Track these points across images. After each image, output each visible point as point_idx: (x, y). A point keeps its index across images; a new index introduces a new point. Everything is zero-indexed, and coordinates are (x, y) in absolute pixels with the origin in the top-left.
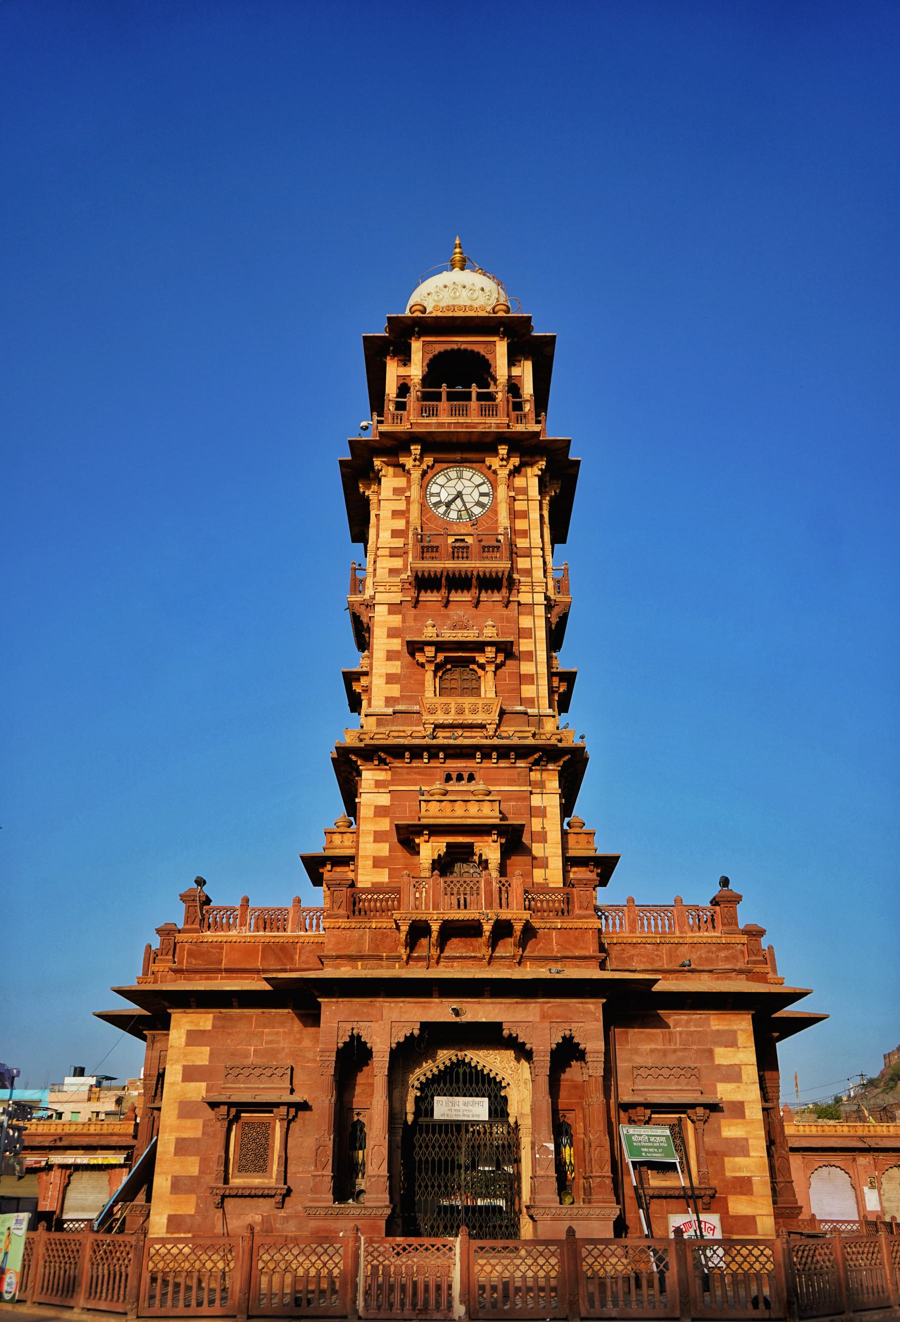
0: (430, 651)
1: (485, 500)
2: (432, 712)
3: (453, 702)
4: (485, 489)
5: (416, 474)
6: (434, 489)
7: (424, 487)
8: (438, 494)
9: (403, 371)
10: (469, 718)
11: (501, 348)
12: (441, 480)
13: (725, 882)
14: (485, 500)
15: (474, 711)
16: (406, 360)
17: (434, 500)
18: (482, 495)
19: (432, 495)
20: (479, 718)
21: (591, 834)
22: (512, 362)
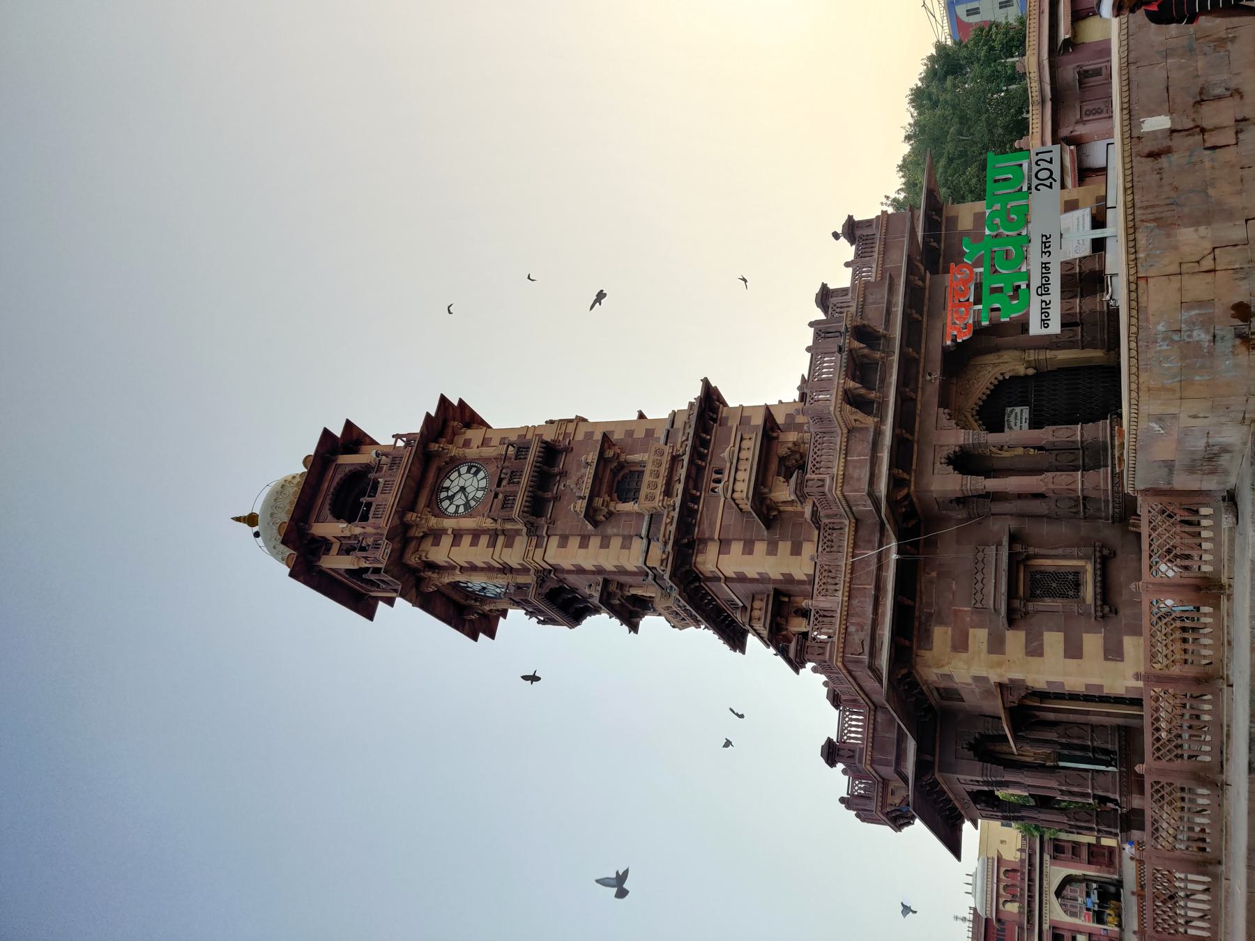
1: (474, 470)
4: (464, 469)
5: (433, 521)
7: (449, 517)
8: (458, 507)
13: (836, 236)
18: (468, 471)
19: (456, 512)
20: (666, 459)
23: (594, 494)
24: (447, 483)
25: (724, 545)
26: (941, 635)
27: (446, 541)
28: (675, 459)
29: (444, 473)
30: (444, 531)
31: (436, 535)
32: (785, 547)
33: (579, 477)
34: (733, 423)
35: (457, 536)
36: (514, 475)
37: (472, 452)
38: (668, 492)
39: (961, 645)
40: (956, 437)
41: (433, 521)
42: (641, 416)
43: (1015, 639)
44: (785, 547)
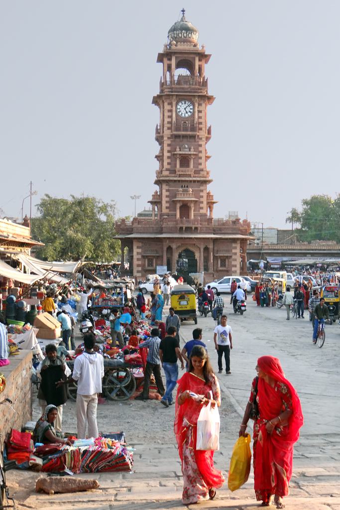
0: (178, 156)
1: (191, 111)
2: (179, 171)
3: (183, 169)
5: (174, 103)
6: (179, 107)
9: (169, 62)
10: (187, 173)
11: (197, 59)
12: (180, 104)
14: (191, 111)
15: (188, 171)
16: (170, 59)
17: (179, 110)
20: (189, 173)
21: (212, 196)
22: (200, 60)
23: (180, 154)
24: (187, 103)
25: (167, 191)
26: (140, 244)
27: (169, 107)
28: (190, 176)
29: (190, 100)
30: (172, 107)
31: (170, 104)
32: (168, 205)
33: (187, 150)
34: (202, 188)
35: (171, 111)
36: (186, 129)
37: (196, 109)
38: (180, 176)
39: (138, 247)
40: (174, 246)
41: (174, 103)
42: (208, 157)
43: (140, 257)
44: (168, 205)
